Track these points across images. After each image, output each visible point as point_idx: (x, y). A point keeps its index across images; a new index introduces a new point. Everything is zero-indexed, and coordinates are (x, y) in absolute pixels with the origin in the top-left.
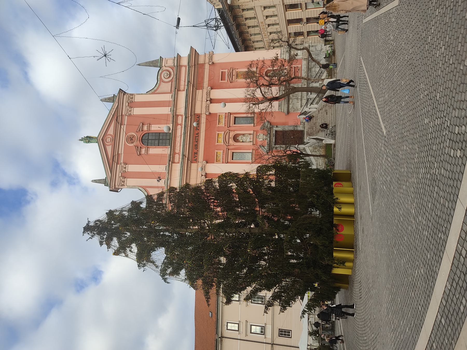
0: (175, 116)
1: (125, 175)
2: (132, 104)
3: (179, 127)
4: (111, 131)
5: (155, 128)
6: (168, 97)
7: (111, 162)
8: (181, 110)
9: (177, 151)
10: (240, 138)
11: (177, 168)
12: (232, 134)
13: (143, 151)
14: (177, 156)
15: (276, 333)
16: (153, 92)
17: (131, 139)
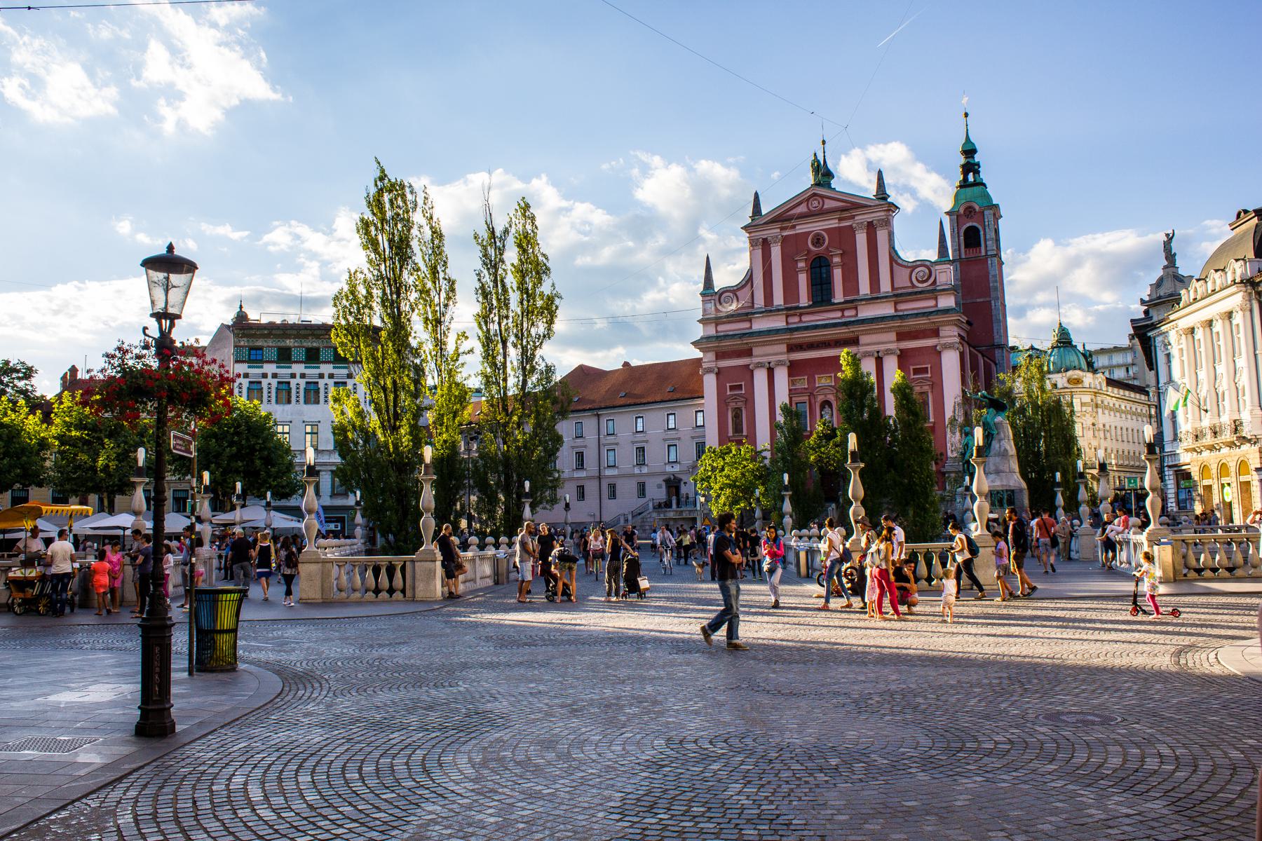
0: (852, 304)
1: (765, 245)
2: (871, 228)
3: (839, 314)
4: (829, 204)
5: (837, 274)
6: (885, 287)
7: (783, 217)
8: (866, 312)
9: (805, 318)
10: (827, 409)
11: (779, 323)
12: (831, 398)
13: (801, 265)
14: (796, 319)
15: (612, 481)
16: (894, 258)
17: (818, 240)
